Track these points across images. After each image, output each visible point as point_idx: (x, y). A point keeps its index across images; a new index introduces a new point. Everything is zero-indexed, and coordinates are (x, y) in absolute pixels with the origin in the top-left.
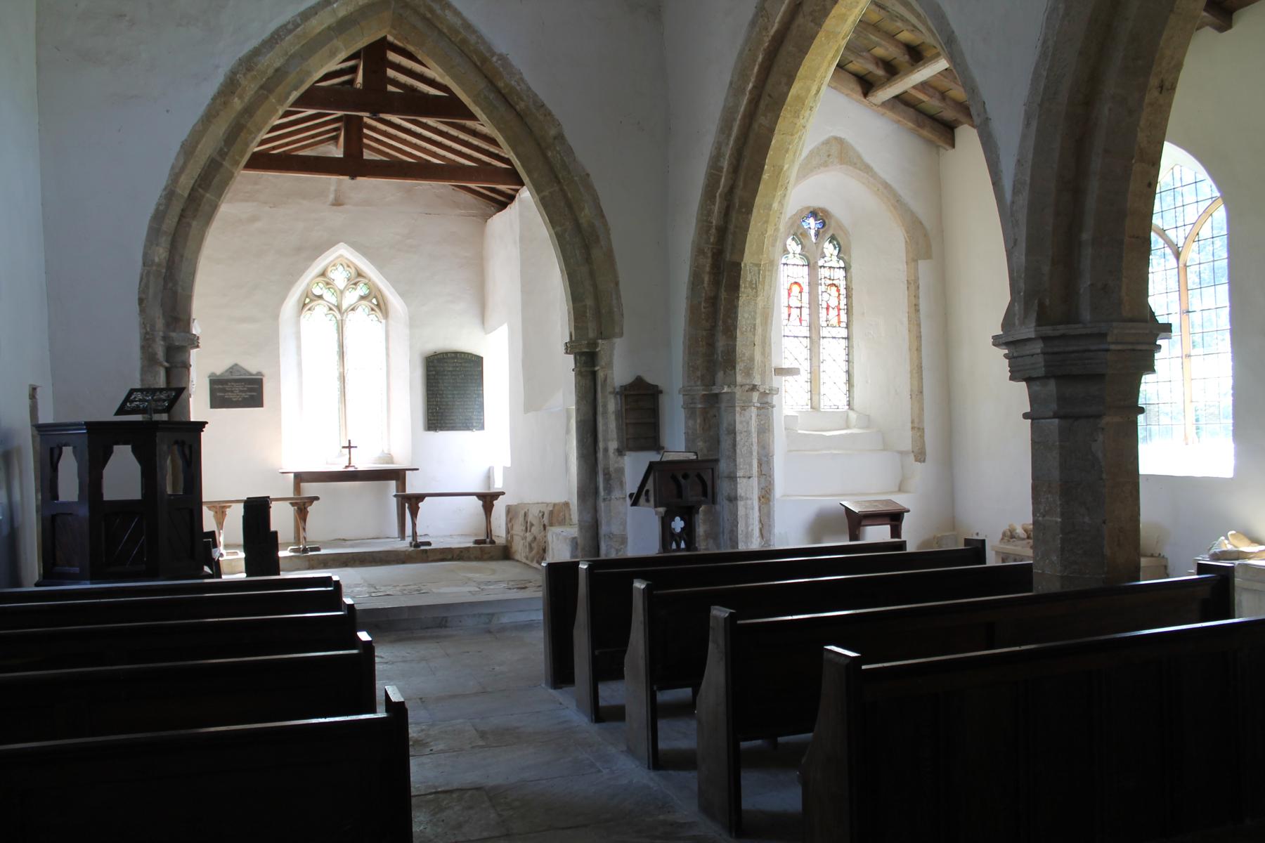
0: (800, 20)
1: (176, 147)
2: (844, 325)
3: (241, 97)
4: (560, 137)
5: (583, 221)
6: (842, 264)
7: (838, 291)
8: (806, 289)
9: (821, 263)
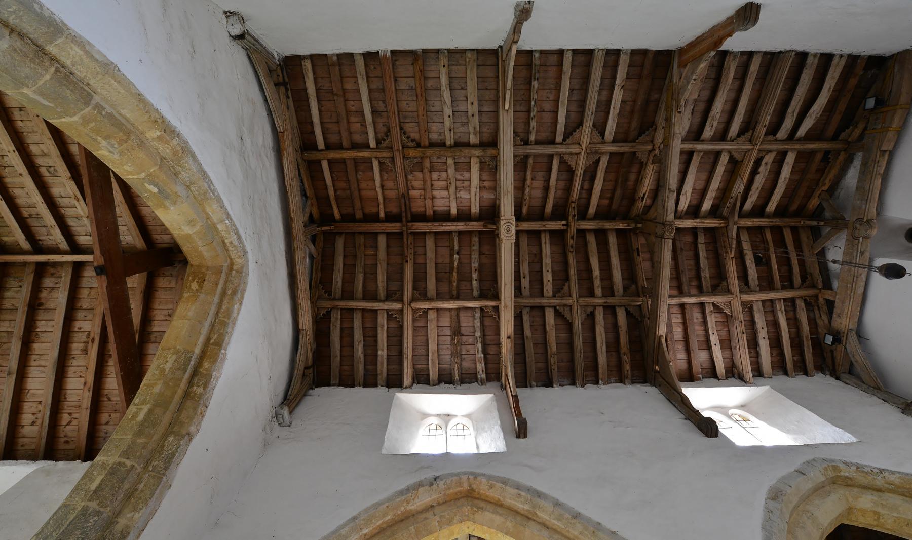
0: (429, 515)
1: (113, 57)
3: (159, 138)
4: (190, 436)
5: (122, 522)
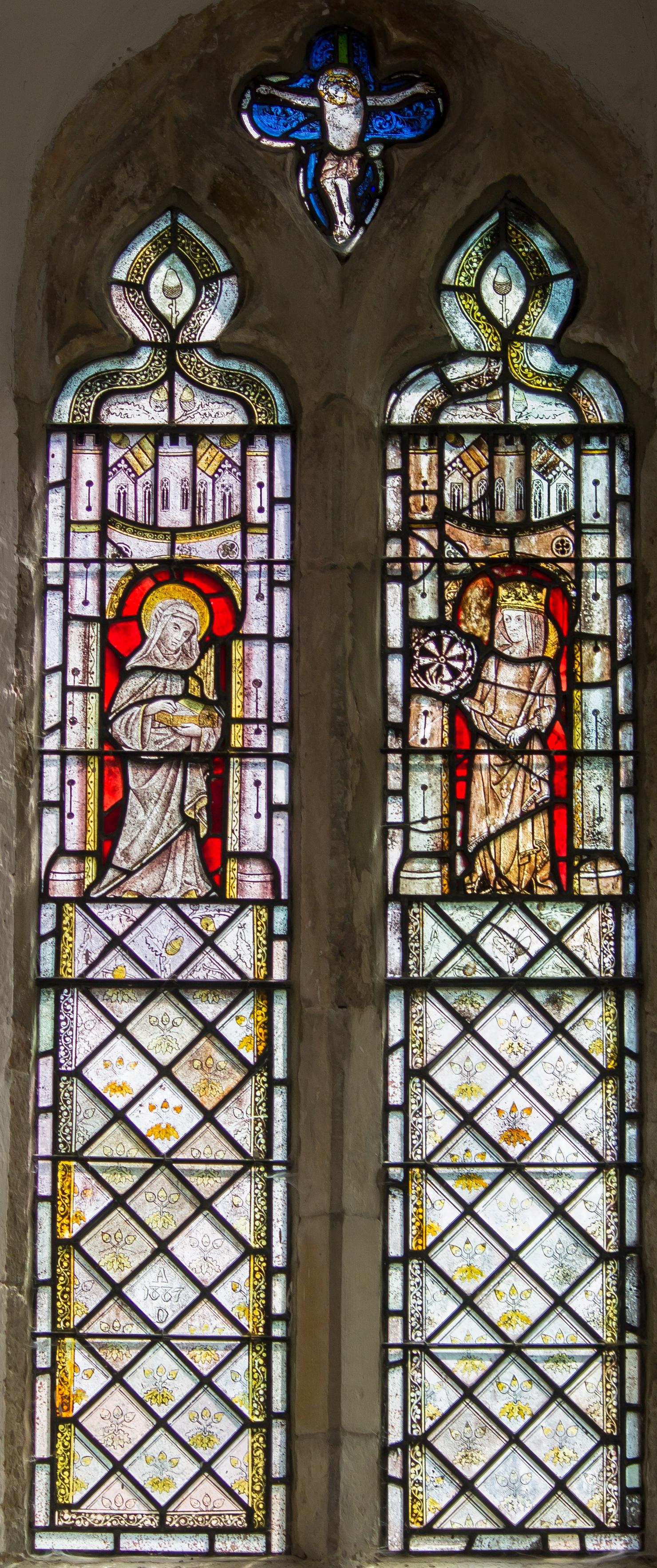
2: (607, 879)
6: (603, 404)
7: (562, 609)
8: (267, 611)
9: (406, 408)
